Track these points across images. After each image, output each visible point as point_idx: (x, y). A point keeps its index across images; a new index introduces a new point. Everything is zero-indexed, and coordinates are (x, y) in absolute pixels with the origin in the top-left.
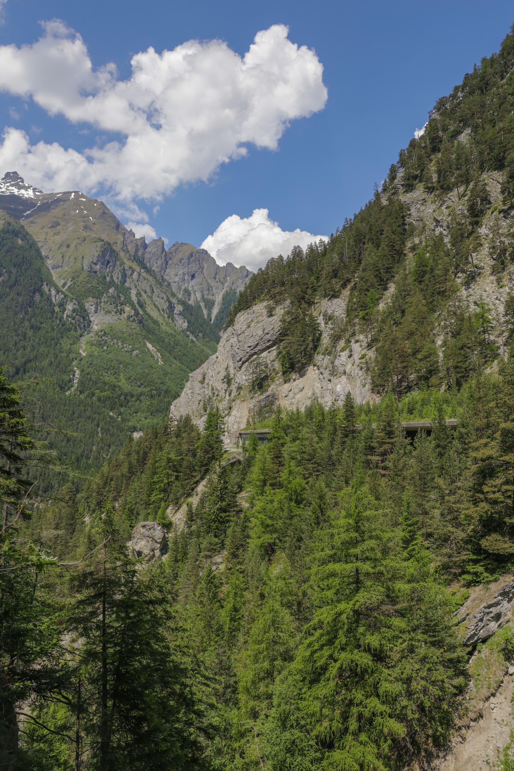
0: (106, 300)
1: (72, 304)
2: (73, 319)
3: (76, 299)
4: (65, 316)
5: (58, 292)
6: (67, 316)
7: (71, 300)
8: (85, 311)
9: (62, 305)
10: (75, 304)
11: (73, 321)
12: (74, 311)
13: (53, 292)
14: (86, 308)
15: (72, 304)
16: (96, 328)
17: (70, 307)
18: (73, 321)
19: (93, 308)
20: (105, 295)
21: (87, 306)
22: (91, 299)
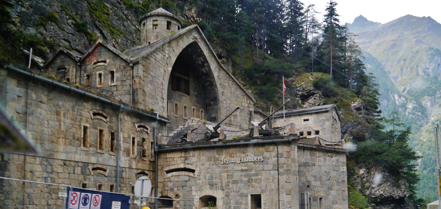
0: (439, 96)
1: (411, 104)
2: (414, 115)
3: (414, 100)
4: (407, 113)
5: (400, 97)
6: (409, 113)
7: (411, 101)
8: (422, 107)
9: (404, 106)
10: (414, 104)
11: (413, 116)
12: (414, 108)
13: (396, 97)
14: (423, 104)
15: (411, 104)
16: (432, 119)
17: (410, 106)
18: (413, 116)
19: (429, 104)
20: (438, 92)
21: (424, 103)
22: (426, 97)
